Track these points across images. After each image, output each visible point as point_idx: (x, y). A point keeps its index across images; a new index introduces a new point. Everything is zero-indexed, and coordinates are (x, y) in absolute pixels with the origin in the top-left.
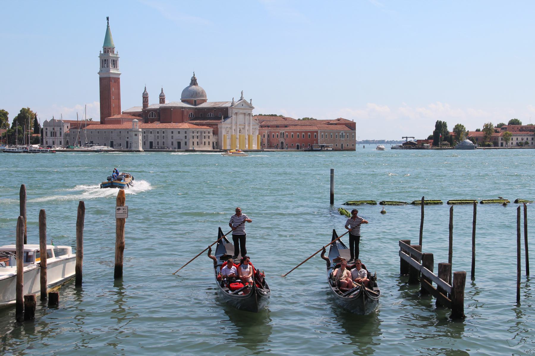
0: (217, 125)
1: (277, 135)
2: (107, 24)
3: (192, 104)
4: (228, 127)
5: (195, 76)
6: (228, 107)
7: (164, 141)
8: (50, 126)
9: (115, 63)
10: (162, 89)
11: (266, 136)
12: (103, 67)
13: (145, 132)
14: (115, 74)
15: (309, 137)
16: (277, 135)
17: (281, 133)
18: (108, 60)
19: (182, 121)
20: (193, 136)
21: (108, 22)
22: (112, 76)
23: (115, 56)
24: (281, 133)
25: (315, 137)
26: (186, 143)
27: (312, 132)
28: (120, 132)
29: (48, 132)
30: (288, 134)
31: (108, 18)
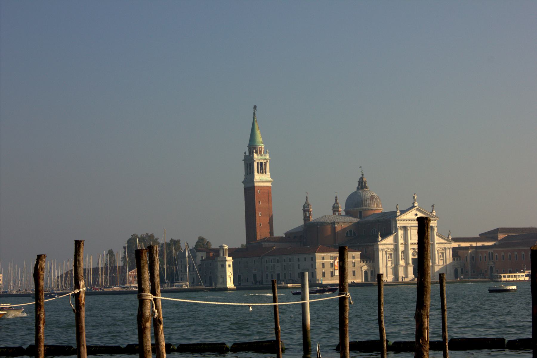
0: (373, 245)
1: (485, 256)
2: (253, 117)
3: (355, 217)
4: (390, 248)
5: (364, 176)
9: (262, 168)
10: (336, 197)
11: (469, 259)
12: (248, 174)
13: (271, 260)
14: (263, 182)
16: (485, 256)
17: (489, 253)
20: (323, 265)
21: (254, 114)
22: (256, 184)
23: (263, 157)
24: (489, 253)
30: (497, 254)
31: (255, 107)
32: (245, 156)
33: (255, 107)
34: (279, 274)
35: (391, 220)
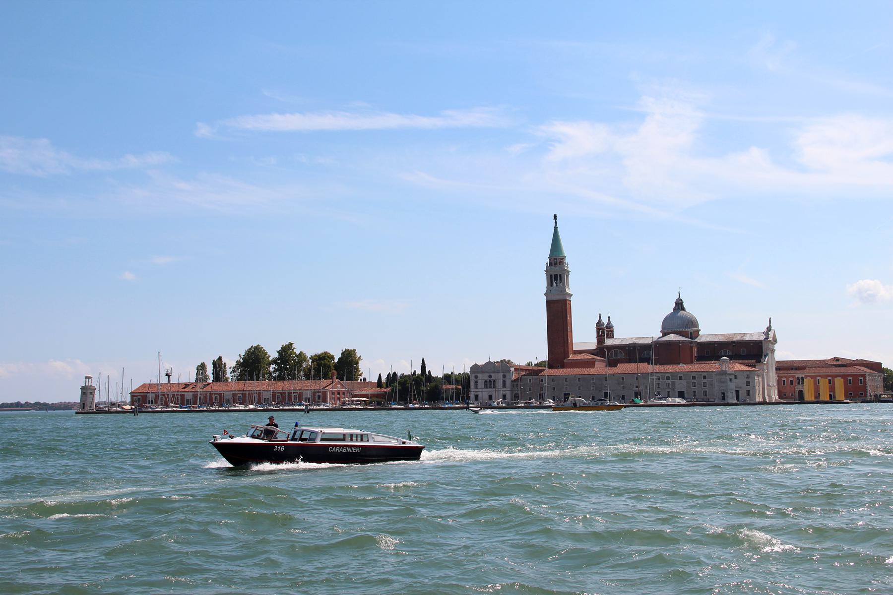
0: (755, 365)
1: (791, 381)
2: (554, 226)
6: (761, 342)
7: (706, 390)
8: (483, 372)
10: (609, 317)
12: (552, 286)
15: (850, 383)
17: (798, 378)
18: (560, 275)
19: (692, 362)
21: (556, 222)
24: (798, 378)
25: (861, 383)
26: (748, 393)
27: (855, 376)
28: (623, 379)
29: (480, 382)
31: (555, 216)
32: (547, 266)
33: (555, 216)
34: (684, 392)
35: (763, 342)
